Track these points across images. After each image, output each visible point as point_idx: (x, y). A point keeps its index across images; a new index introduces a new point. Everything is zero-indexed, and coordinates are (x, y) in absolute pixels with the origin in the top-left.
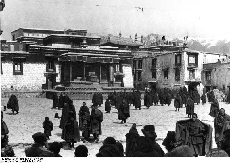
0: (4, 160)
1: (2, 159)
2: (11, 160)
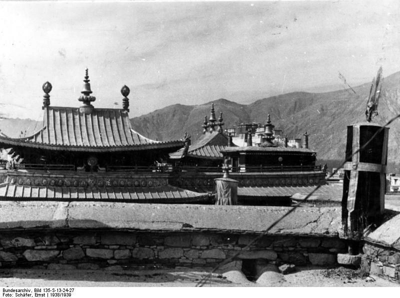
0: (7, 293)
1: (4, 290)
2: (19, 293)
